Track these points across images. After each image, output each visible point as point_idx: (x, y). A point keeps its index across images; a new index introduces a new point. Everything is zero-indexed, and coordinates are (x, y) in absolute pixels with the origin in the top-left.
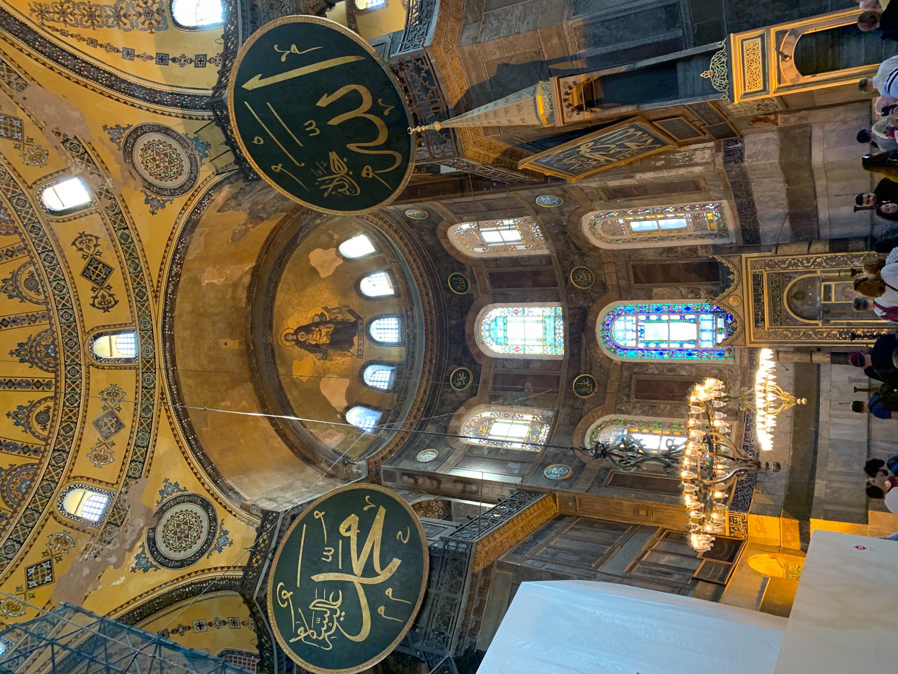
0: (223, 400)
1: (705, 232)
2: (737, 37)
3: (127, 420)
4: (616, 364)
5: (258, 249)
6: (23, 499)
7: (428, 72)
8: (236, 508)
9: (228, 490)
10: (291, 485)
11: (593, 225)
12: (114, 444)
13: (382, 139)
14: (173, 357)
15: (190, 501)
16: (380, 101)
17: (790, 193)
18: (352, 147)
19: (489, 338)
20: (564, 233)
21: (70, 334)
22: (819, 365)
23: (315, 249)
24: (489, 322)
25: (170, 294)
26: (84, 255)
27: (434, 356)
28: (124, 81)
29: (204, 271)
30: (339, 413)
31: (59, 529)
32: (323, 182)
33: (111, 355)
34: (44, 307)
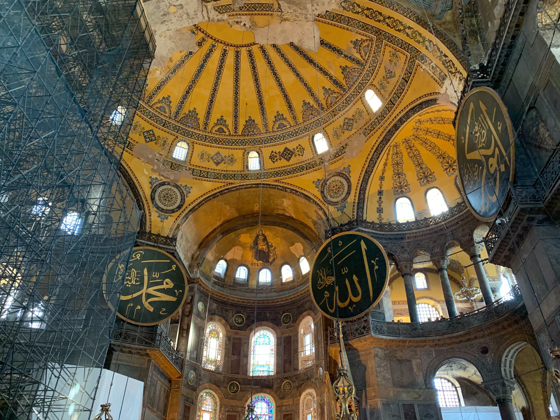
0: (230, 206)
3: (219, 167)
4: (244, 404)
5: (301, 220)
6: (184, 125)
7: (363, 333)
8: (178, 222)
9: (186, 216)
10: (189, 242)
11: (310, 394)
13: (340, 304)
14: (249, 188)
15: (182, 199)
16: (354, 305)
20: (308, 379)
28: (369, 177)
29: (289, 199)
31: (169, 142)
32: (323, 272)
34: (271, 130)
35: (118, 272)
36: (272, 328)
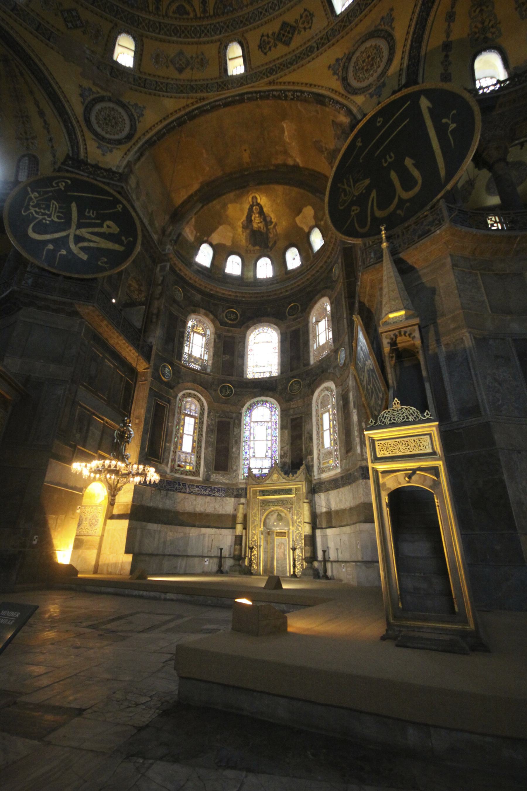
1: (321, 460)
2: (434, 429)
4: (240, 409)
11: (327, 389)
12: (167, 67)
13: (378, 214)
17: (343, 511)
18: (374, 194)
19: (258, 333)
20: (323, 372)
21: (242, 22)
22: (234, 528)
23: (314, 209)
24: (268, 332)
25: (272, 94)
26: (297, 21)
27: (247, 299)
30: (208, 239)
33: (230, 59)
35: (29, 202)
36: (276, 324)
